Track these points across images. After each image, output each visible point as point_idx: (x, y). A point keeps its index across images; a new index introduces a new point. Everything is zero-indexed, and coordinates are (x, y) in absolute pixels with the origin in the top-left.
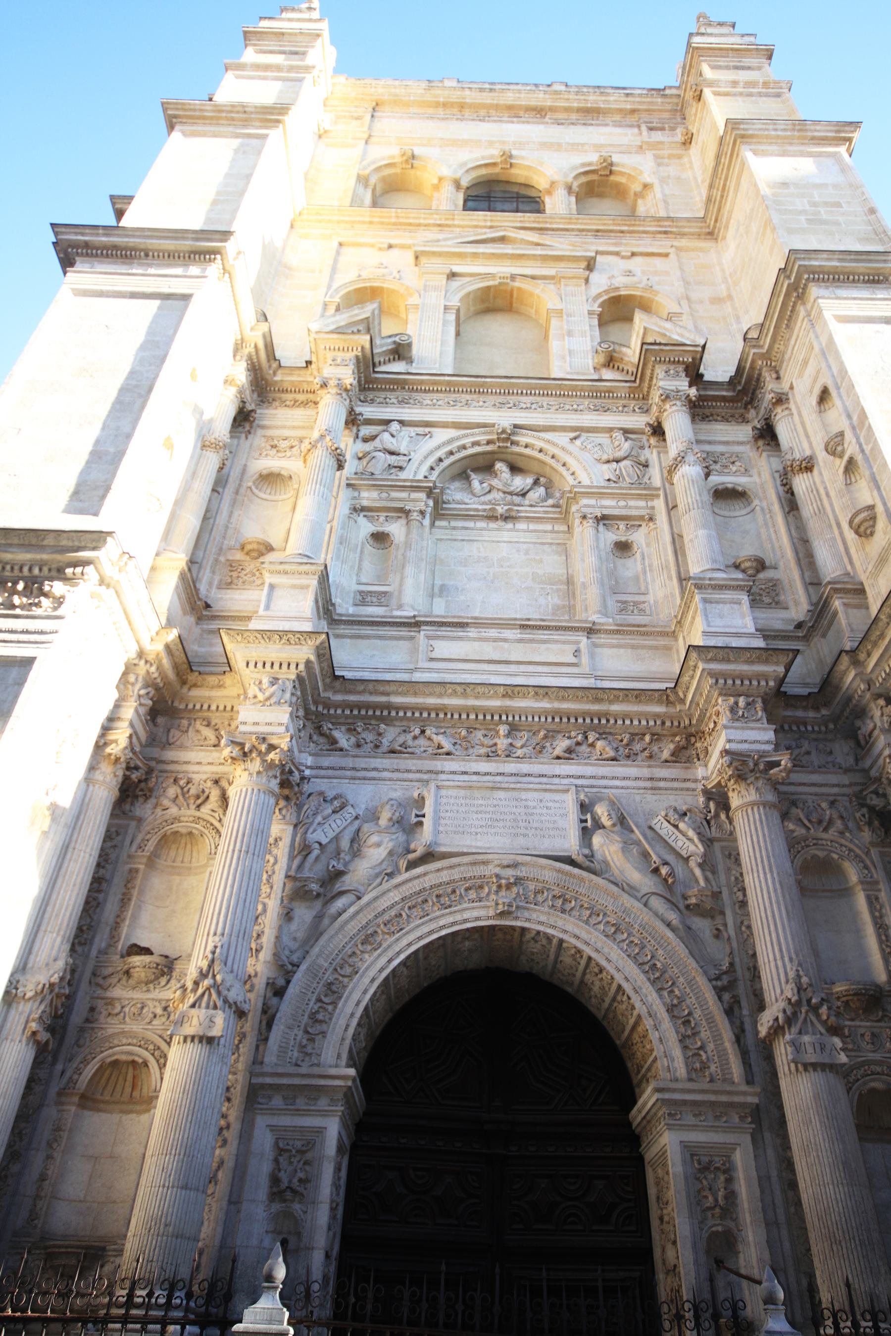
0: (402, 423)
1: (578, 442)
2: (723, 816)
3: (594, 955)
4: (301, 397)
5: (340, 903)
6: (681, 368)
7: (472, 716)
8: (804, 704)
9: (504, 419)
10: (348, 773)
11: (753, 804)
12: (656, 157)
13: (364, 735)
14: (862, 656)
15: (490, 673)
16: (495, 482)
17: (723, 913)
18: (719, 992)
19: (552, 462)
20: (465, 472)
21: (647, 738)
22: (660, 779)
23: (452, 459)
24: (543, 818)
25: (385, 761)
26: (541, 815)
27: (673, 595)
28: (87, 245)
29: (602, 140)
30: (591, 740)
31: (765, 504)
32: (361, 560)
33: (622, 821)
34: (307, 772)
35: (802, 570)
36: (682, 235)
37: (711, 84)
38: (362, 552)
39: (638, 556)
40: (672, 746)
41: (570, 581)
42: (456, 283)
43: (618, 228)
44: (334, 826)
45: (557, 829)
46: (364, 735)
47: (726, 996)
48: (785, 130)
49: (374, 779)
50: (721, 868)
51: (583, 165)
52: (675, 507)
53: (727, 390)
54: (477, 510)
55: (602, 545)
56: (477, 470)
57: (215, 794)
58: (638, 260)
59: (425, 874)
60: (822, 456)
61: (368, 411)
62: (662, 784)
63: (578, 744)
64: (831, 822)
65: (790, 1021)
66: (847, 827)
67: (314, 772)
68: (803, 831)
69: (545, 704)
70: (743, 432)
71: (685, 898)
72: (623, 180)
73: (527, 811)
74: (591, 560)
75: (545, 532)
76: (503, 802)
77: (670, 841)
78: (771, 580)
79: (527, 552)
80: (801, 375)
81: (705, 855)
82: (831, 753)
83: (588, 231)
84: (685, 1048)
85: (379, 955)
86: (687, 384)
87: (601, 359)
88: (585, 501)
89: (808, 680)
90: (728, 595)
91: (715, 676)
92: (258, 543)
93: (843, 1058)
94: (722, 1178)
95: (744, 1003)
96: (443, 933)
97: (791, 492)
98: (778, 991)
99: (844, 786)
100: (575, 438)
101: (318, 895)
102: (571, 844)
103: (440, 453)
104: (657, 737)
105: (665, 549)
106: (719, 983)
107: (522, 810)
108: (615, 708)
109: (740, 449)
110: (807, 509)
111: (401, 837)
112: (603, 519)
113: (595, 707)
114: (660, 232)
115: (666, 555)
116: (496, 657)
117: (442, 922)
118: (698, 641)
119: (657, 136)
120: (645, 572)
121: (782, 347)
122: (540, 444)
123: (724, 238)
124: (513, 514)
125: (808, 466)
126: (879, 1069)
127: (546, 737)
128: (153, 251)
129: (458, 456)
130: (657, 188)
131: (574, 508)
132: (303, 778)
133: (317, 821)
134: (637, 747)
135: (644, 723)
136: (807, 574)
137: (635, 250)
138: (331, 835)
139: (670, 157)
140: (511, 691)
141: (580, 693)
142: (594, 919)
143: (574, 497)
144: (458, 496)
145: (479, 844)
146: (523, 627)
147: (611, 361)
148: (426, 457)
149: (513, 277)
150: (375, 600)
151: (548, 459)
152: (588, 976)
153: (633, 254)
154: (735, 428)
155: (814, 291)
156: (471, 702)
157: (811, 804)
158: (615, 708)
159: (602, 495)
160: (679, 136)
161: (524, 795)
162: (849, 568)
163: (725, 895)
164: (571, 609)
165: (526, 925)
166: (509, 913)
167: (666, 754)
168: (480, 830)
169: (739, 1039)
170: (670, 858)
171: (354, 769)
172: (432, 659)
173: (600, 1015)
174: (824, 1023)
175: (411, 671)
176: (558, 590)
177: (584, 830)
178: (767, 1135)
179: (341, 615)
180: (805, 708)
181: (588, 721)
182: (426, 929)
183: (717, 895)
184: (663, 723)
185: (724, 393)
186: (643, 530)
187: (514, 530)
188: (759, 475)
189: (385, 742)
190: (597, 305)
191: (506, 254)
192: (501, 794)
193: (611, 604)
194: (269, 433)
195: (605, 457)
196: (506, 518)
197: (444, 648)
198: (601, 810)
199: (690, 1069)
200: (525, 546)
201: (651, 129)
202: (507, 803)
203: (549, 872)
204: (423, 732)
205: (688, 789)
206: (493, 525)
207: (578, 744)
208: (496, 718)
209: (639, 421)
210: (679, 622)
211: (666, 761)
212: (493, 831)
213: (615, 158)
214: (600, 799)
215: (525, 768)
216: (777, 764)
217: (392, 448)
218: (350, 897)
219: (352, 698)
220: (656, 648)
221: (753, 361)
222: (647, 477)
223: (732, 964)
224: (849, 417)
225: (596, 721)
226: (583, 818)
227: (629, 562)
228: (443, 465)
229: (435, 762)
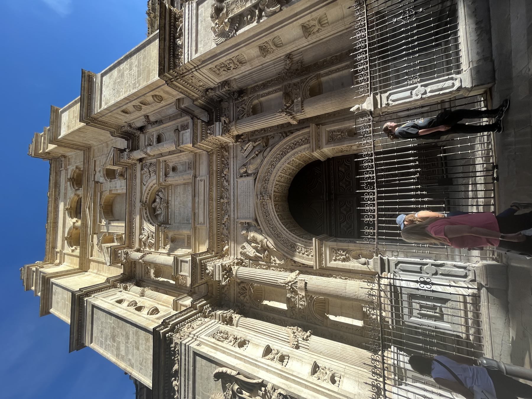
1: (145, 183)
2: (242, 137)
3: (280, 171)
4: (133, 266)
6: (121, 154)
7: (219, 210)
9: (138, 205)
11: (236, 128)
12: (69, 165)
14: (194, 98)
15: (207, 206)
16: (158, 207)
17: (267, 136)
18: (287, 136)
19: (151, 190)
20: (155, 216)
21: (223, 159)
23: (150, 220)
27: (185, 154)
28: (78, 340)
29: (64, 181)
31: (161, 130)
33: (244, 165)
34: (235, 258)
35: (178, 118)
37: (44, 149)
39: (176, 165)
40: (225, 152)
41: (185, 184)
48: (53, 127)
50: (256, 137)
51: (70, 186)
53: (130, 141)
54: (165, 212)
55: (173, 175)
56: (155, 213)
57: (242, 285)
58: (96, 169)
59: (260, 221)
60: (143, 112)
61: (137, 246)
62: (235, 155)
63: (225, 179)
64: (243, 108)
65: (291, 115)
66: (244, 103)
67: (236, 255)
69: (214, 189)
70: (142, 136)
71: (264, 147)
72: (76, 174)
74: (177, 178)
78: (181, 128)
81: (252, 141)
82: (225, 109)
83: (87, 184)
84: (302, 145)
85: (283, 233)
87: (121, 178)
88: (161, 180)
90: (181, 137)
91: (202, 139)
93: (299, 99)
94: (334, 133)
95: (290, 129)
97: (156, 122)
98: (284, 118)
102: (251, 179)
104: (223, 157)
105: (173, 157)
106: (285, 136)
107: (243, 194)
108: (215, 169)
109: (147, 137)
110: (159, 117)
111: (251, 228)
112: (166, 175)
113: (215, 174)
114: (88, 163)
115: (175, 157)
116: (203, 204)
117: (273, 215)
118: (192, 145)
119: (63, 165)
120: (180, 163)
121: (114, 125)
122: (146, 194)
123: (90, 145)
124: (166, 201)
125: (147, 117)
126: (304, 93)
127: (223, 188)
128: (79, 318)
130: (77, 164)
131: (163, 184)
132: (237, 259)
134: (225, 162)
135: (219, 161)
136: (178, 117)
139: (69, 161)
140: (210, 199)
141: (210, 179)
142: (270, 172)
143: (160, 184)
144: (162, 217)
147: (122, 175)
149: (100, 205)
151: (150, 192)
152: (287, 173)
155: (93, 115)
156: (214, 210)
158: (215, 169)
159: (159, 176)
160: (63, 159)
161: (239, 194)
162: (173, 104)
163: (263, 136)
164: (191, 183)
165: (273, 191)
166: (270, 196)
167: (227, 154)
169: (298, 130)
172: (204, 222)
173: (298, 170)
174: (291, 105)
177: (247, 176)
178: (323, 122)
180: (213, 116)
181: (219, 176)
183: (263, 138)
184: (219, 155)
186: (169, 163)
187: (171, 201)
188: (153, 132)
192: (239, 200)
193: (188, 172)
194: (143, 275)
195: (149, 175)
196: (168, 203)
197: (201, 219)
198: (242, 171)
199: (307, 143)
200: (176, 198)
201: (61, 167)
203: (259, 185)
204: (224, 224)
207: (225, 179)
208: (219, 203)
209: (139, 166)
210: (191, 152)
213: (69, 177)
214: (239, 172)
215: (232, 194)
216: (225, 121)
218: (268, 242)
220: (199, 158)
224: (127, 103)
225: (219, 174)
227: (178, 167)
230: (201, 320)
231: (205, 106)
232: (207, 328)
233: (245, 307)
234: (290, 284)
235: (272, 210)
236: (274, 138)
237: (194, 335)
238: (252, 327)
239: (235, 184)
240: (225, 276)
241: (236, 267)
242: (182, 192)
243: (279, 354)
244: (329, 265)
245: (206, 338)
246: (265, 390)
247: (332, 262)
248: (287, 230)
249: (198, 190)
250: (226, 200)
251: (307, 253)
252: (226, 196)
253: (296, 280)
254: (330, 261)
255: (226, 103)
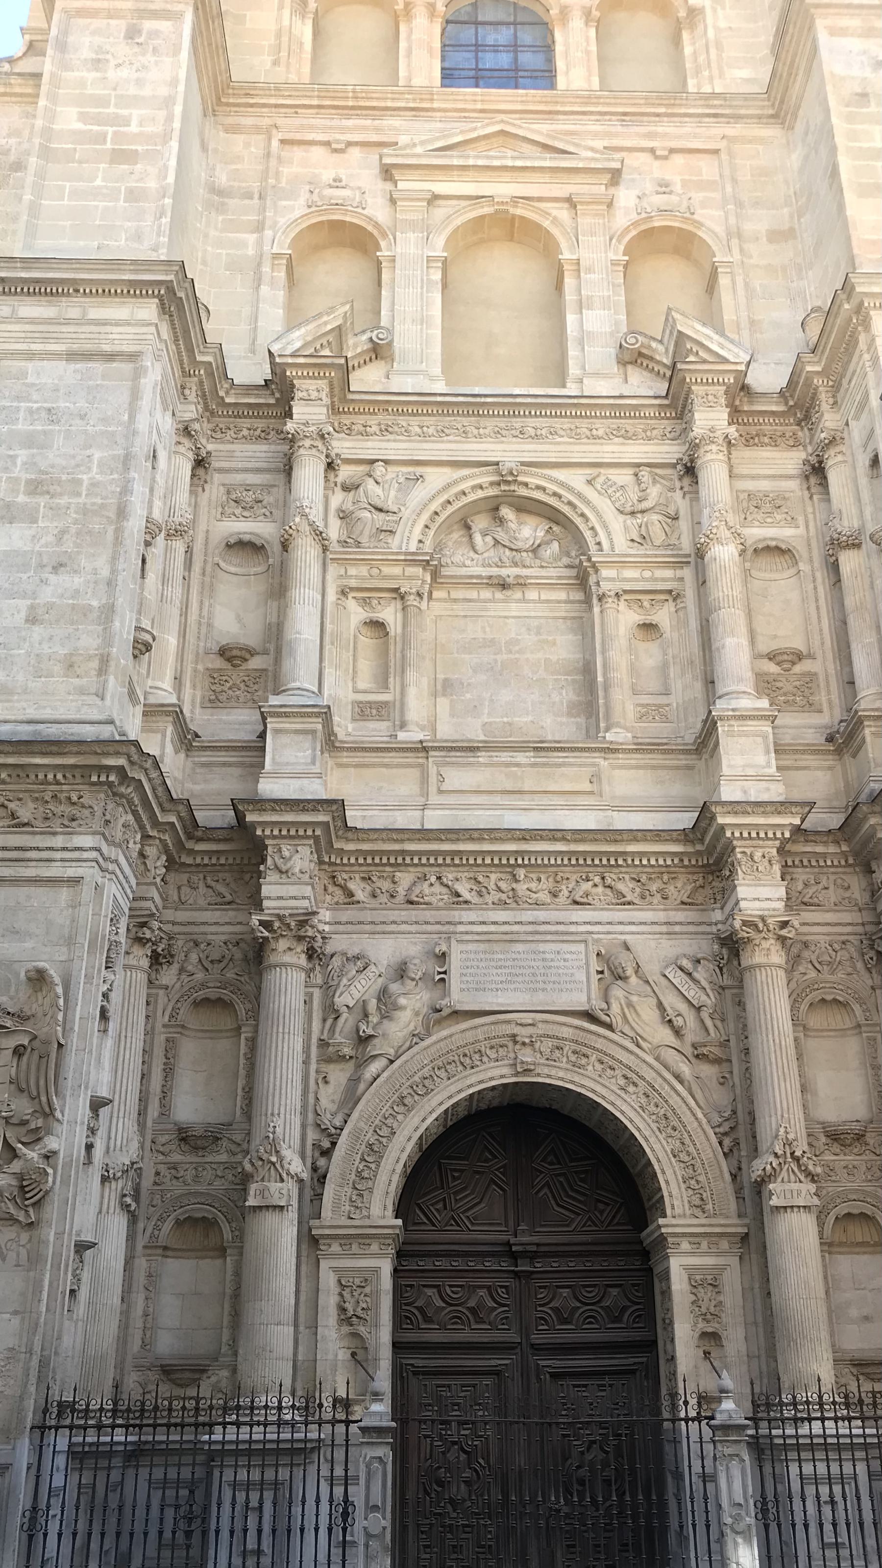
0: (386, 462)
5: (373, 1068)
8: (825, 839)
10: (368, 928)
13: (380, 883)
22: (677, 923)
23: (450, 509)
24: (561, 971)
25: (403, 913)
26: (558, 967)
30: (609, 881)
32: (355, 660)
34: (327, 928)
36: (738, 118)
38: (355, 648)
40: (689, 888)
42: (440, 212)
43: (652, 110)
44: (359, 986)
45: (575, 982)
46: (378, 884)
47: (727, 1142)
49: (393, 933)
52: (704, 582)
53: (777, 403)
54: (479, 577)
58: (678, 160)
59: (451, 1036)
62: (677, 928)
63: (596, 885)
66: (855, 968)
68: (813, 974)
73: (545, 964)
75: (559, 602)
76: (522, 956)
77: (683, 990)
79: (538, 633)
80: (857, 418)
86: (726, 416)
89: (835, 804)
92: (241, 649)
95: (743, 1145)
96: (471, 1091)
99: (857, 924)
100: (594, 479)
101: (351, 1057)
103: (434, 506)
106: (721, 1130)
107: (540, 964)
108: (632, 848)
117: (468, 1082)
124: (522, 581)
129: (457, 505)
132: (323, 938)
133: (342, 984)
134: (654, 887)
137: (674, 144)
138: (357, 995)
145: (500, 1000)
146: (536, 749)
148: (419, 515)
149: (516, 200)
150: (374, 712)
153: (672, 151)
154: (786, 454)
157: (823, 945)
158: (632, 848)
161: (542, 947)
163: (733, 1043)
168: (500, 986)
170: (682, 1007)
171: (372, 923)
175: (424, 807)
176: (574, 681)
179: (342, 742)
180: (825, 843)
182: (453, 1089)
185: (774, 408)
187: (524, 600)
189: (401, 890)
190: (622, 248)
191: (506, 167)
192: (520, 947)
195: (628, 509)
200: (536, 623)
202: (525, 956)
205: (703, 933)
206: (499, 595)
209: (670, 452)
211: (683, 903)
212: (512, 986)
217: (379, 504)
218: (383, 1062)
219: (365, 847)
220: (677, 768)
221: (807, 379)
222: (676, 535)
223: (734, 1112)
226: (600, 969)
228: (440, 520)
229: (453, 912)
230: (135, 843)
231: (857, 830)
232: (124, 881)
233: (165, 967)
234: (274, 1159)
235: (481, 1077)
236: (722, 1084)
237: (116, 861)
238: (130, 1021)
239: (573, 928)
240: (277, 924)
241: (303, 960)
242: (554, 658)
243: (91, 1139)
244: (324, 1265)
245: (111, 902)
246: (38, 1129)
247: (332, 1274)
248: (422, 1130)
249: (560, 765)
250: (521, 888)
251: (354, 1198)
252: (533, 886)
253: (284, 1175)
254: (335, 1270)
255: (867, 896)
